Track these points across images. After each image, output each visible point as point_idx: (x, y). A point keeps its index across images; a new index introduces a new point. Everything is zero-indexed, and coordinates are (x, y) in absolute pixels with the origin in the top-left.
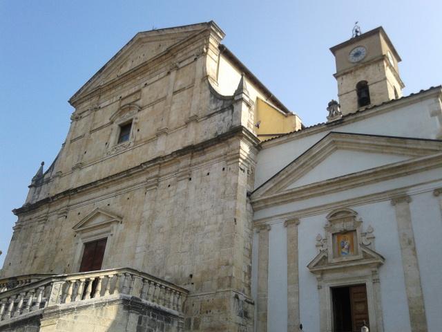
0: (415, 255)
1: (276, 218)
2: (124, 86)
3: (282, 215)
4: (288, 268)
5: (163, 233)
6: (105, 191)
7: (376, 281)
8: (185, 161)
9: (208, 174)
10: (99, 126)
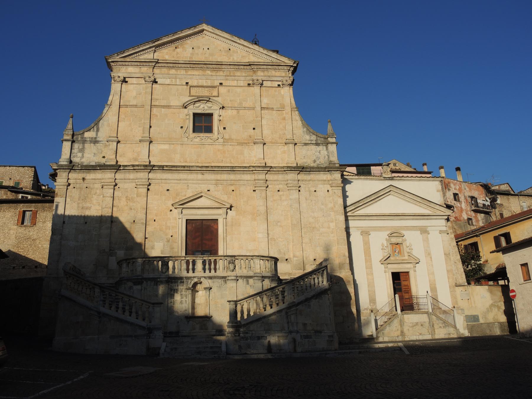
0: (431, 260)
1: (353, 228)
2: (190, 73)
3: (358, 227)
4: (365, 259)
5: (281, 226)
6: (200, 176)
7: (415, 271)
8: (292, 176)
9: (315, 191)
10: (164, 103)
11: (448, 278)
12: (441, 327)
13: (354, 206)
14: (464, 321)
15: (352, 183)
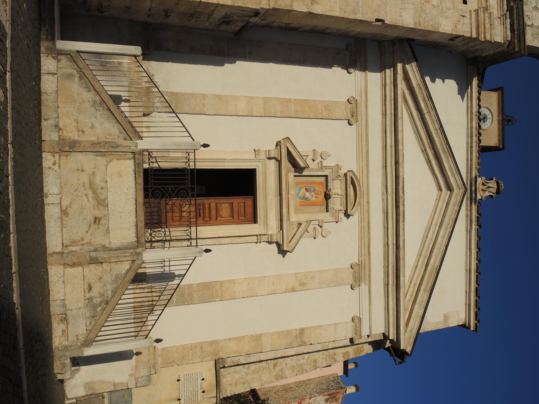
3: (366, 93)
4: (289, 101)
11: (239, 339)
12: (90, 288)
13: (419, 85)
14: (115, 385)
15: (459, 97)
